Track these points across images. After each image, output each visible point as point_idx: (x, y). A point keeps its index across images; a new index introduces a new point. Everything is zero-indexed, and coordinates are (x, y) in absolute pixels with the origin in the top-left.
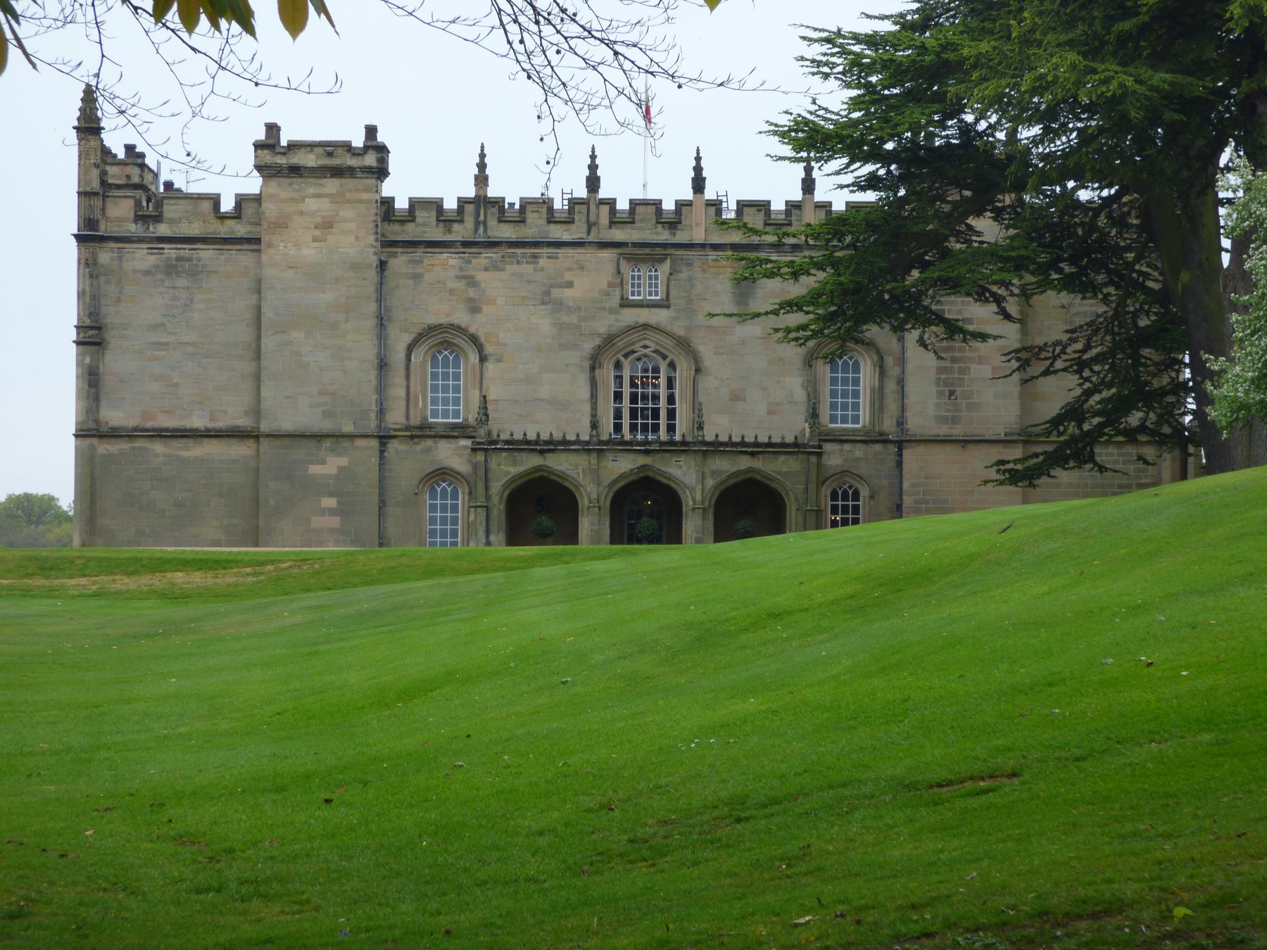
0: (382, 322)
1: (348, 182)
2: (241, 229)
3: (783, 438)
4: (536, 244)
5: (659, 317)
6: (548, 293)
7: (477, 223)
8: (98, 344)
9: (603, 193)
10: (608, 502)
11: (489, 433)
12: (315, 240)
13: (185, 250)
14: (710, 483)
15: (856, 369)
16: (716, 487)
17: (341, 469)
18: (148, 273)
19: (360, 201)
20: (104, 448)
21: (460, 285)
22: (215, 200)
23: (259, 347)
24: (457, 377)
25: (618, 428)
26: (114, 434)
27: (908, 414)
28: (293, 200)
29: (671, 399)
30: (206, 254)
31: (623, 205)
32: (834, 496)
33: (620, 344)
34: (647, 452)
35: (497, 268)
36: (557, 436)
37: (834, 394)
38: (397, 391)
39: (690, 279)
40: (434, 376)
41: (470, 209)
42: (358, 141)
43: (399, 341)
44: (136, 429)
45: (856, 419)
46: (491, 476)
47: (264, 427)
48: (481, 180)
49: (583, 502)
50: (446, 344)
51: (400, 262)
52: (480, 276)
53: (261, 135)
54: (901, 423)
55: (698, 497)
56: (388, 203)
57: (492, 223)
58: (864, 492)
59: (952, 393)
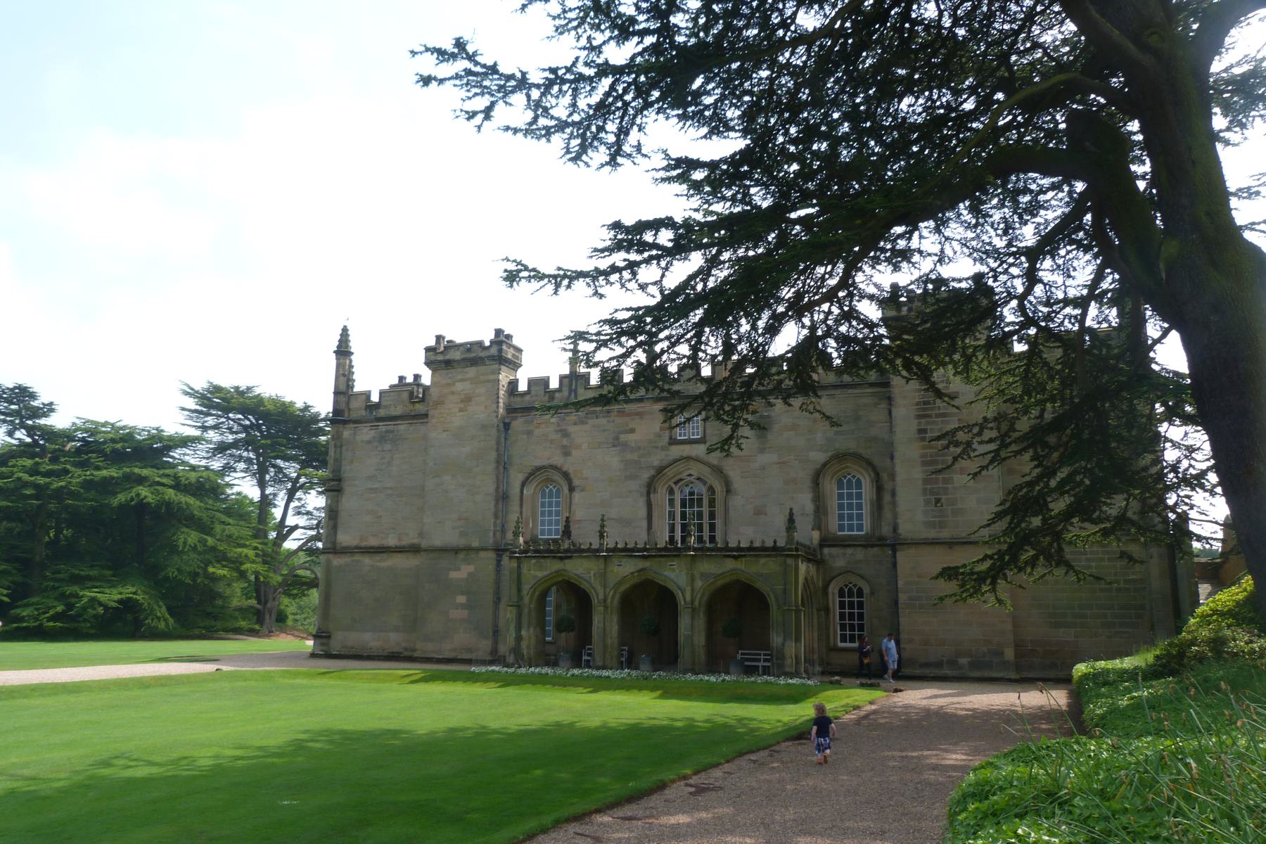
0: (503, 465)
1: (482, 369)
2: (420, 408)
3: (763, 542)
6: (617, 438)
8: (339, 491)
10: (616, 602)
13: (390, 426)
14: (699, 583)
17: (470, 574)
18: (369, 442)
19: (488, 381)
20: (337, 561)
21: (559, 436)
26: (346, 551)
27: (899, 521)
28: (448, 384)
29: (712, 516)
30: (403, 427)
32: (841, 594)
33: (670, 472)
35: (583, 423)
37: (841, 507)
38: (513, 517)
40: (543, 505)
43: (517, 478)
44: (356, 547)
45: (860, 528)
46: (523, 579)
47: (424, 544)
49: (595, 601)
50: (549, 481)
51: (518, 424)
52: (571, 429)
53: (432, 343)
54: (895, 529)
55: (688, 598)
56: (513, 384)
57: (581, 391)
58: (866, 590)
59: (938, 501)
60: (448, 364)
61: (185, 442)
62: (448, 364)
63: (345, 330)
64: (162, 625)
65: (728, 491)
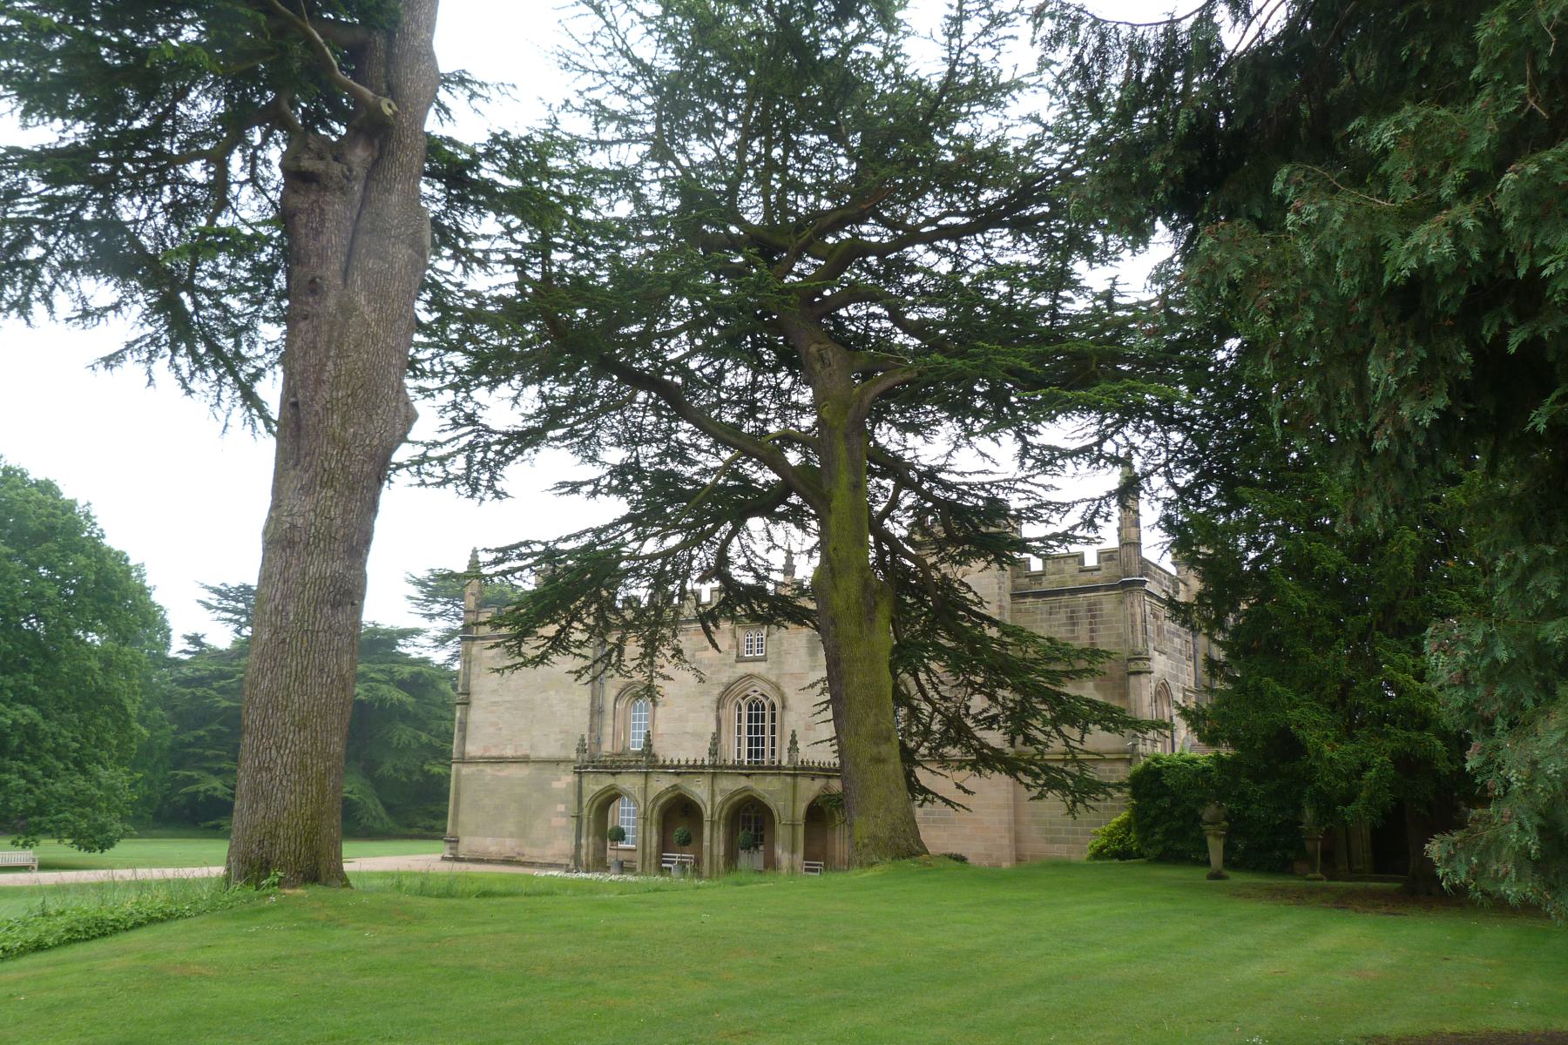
5: (758, 668)
14: (719, 799)
16: (723, 803)
29: (773, 728)
34: (678, 774)
38: (608, 730)
39: (780, 639)
47: (533, 756)
61: (405, 634)
64: (377, 825)
65: (784, 707)
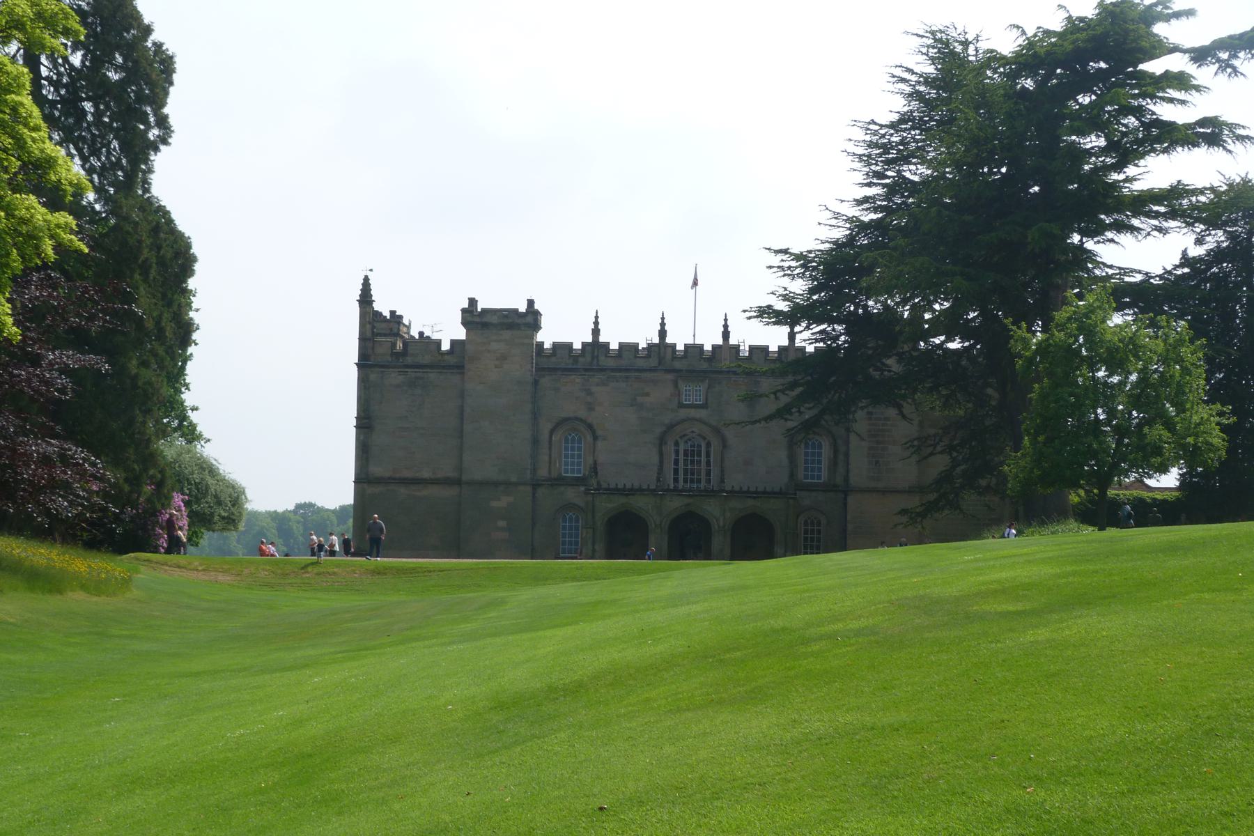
0: (535, 416)
2: (452, 360)
4: (627, 370)
5: (702, 414)
7: (593, 358)
9: (669, 340)
11: (599, 483)
12: (496, 367)
15: (820, 447)
20: (370, 490)
22: (438, 343)
23: (462, 431)
24: (579, 449)
25: (676, 480)
26: (379, 481)
29: (708, 463)
30: (433, 376)
31: (680, 347)
32: (806, 523)
36: (636, 486)
40: (566, 449)
41: (588, 348)
42: (523, 308)
43: (546, 427)
45: (819, 477)
48: (596, 332)
51: (546, 381)
52: (594, 389)
54: (846, 479)
57: (602, 358)
59: (877, 462)
60: (485, 325)
62: (485, 325)
63: (366, 283)
